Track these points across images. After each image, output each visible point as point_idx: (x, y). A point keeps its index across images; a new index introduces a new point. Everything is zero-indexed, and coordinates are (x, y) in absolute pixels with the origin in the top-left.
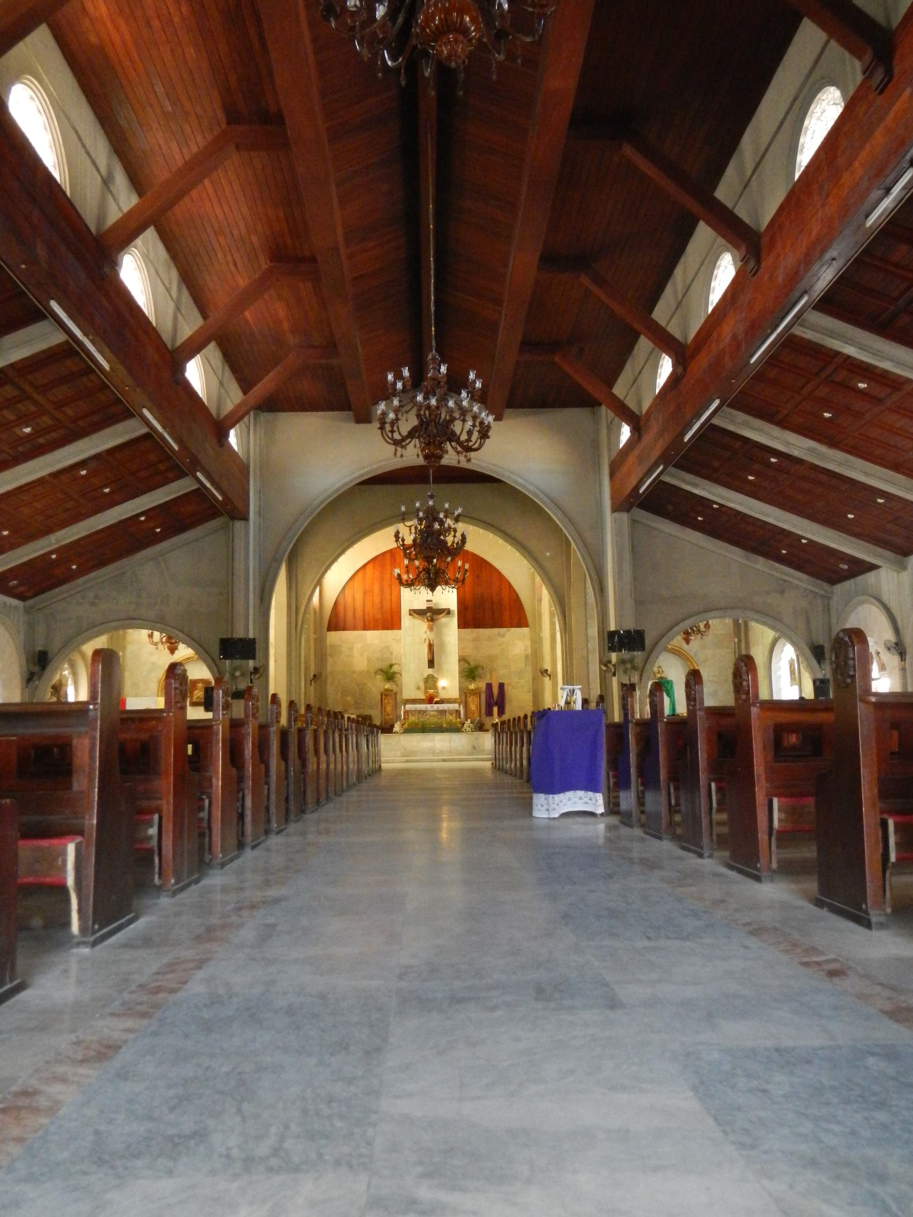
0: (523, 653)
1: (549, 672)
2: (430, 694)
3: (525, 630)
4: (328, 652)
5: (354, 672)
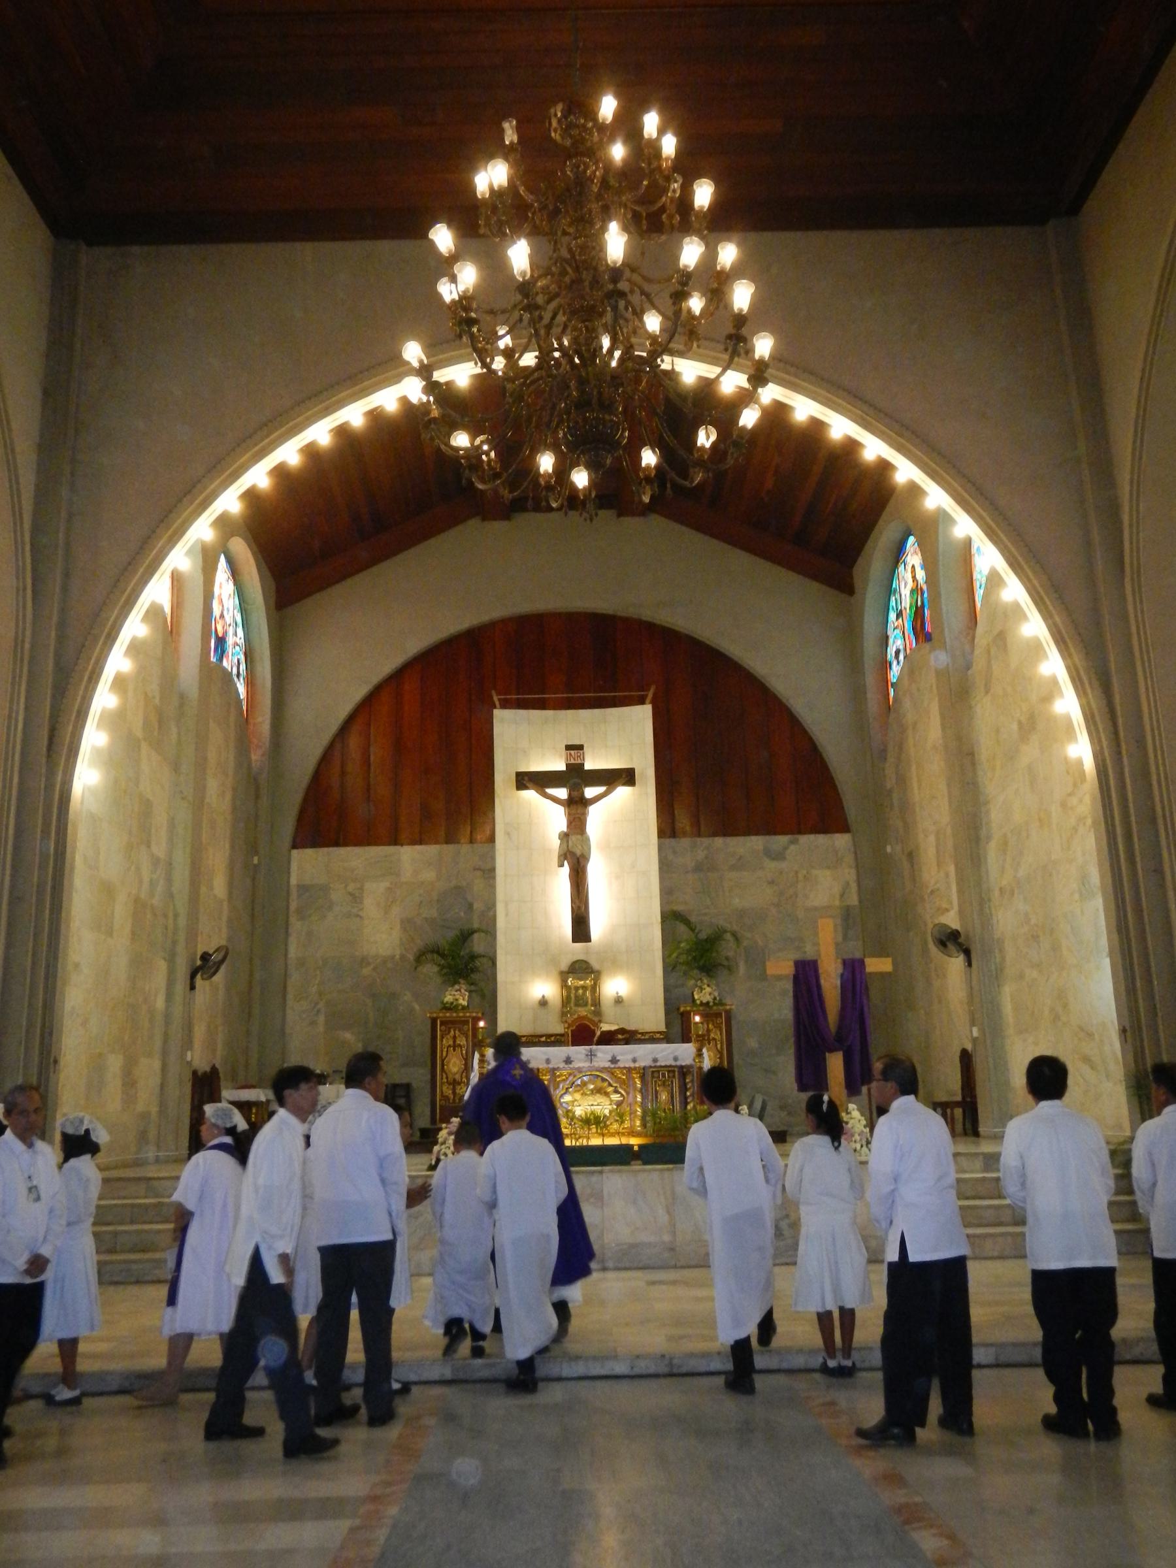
0: (837, 903)
1: (961, 940)
2: (580, 1018)
3: (841, 840)
4: (293, 905)
5: (364, 961)
